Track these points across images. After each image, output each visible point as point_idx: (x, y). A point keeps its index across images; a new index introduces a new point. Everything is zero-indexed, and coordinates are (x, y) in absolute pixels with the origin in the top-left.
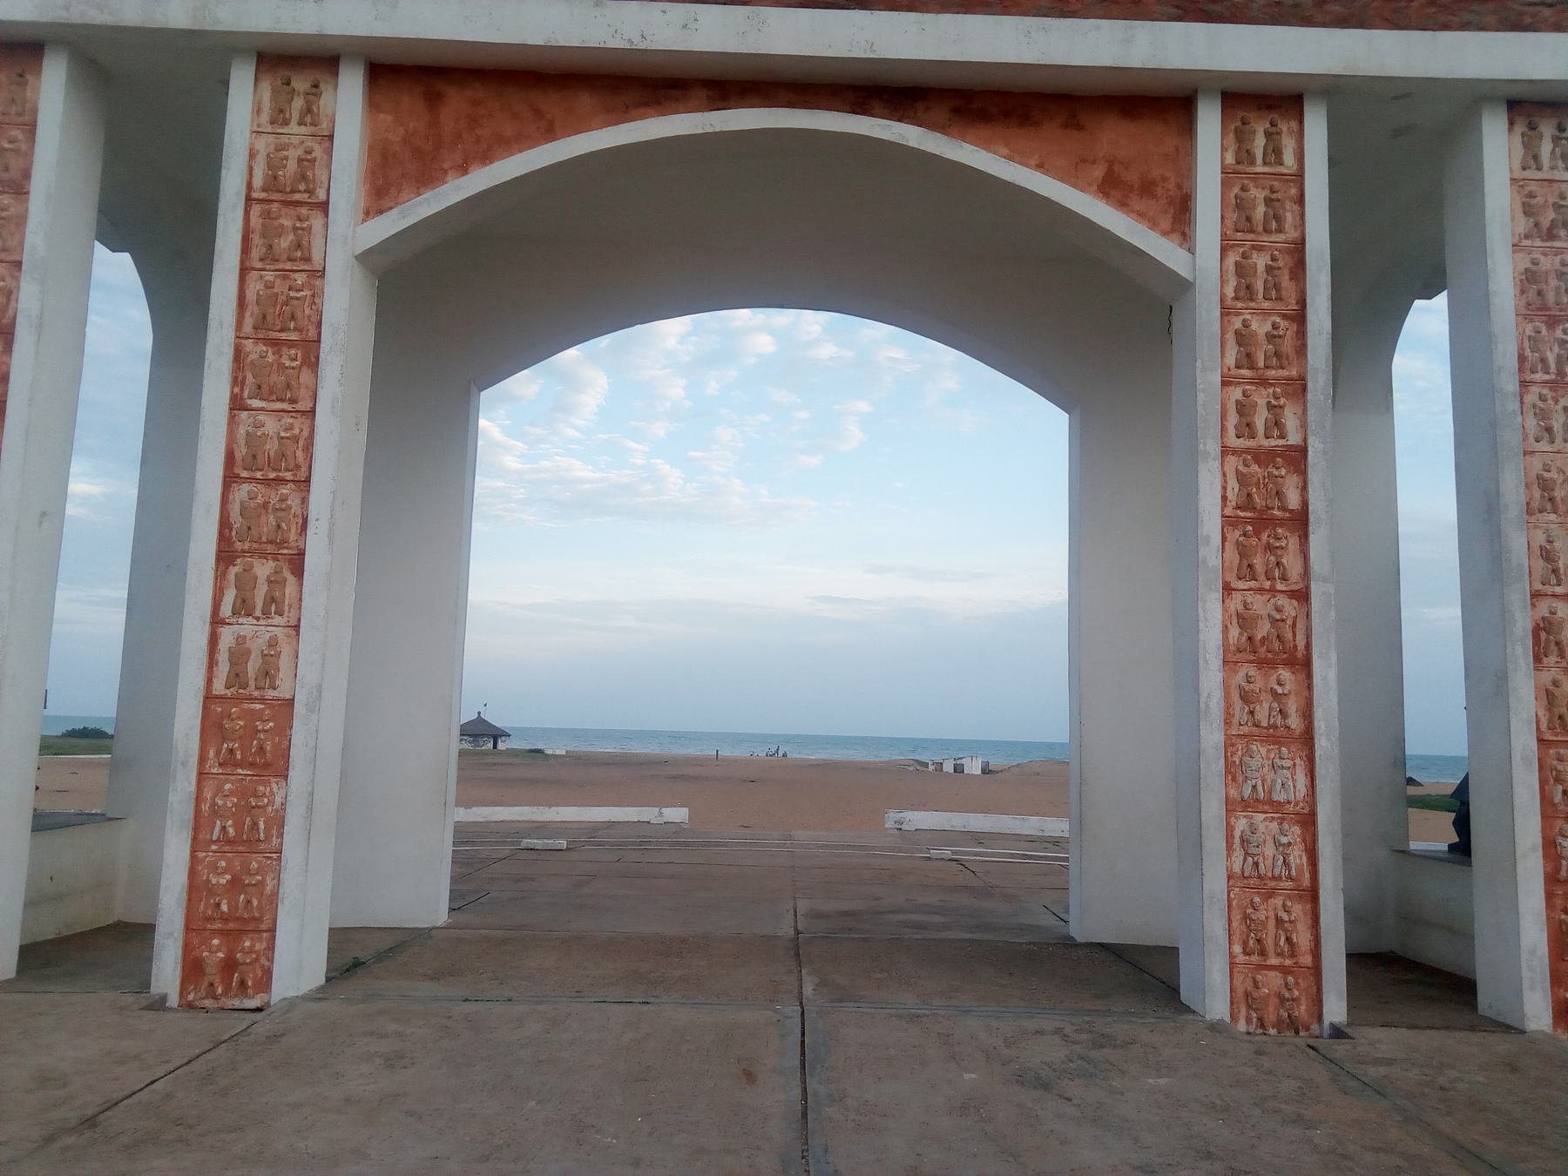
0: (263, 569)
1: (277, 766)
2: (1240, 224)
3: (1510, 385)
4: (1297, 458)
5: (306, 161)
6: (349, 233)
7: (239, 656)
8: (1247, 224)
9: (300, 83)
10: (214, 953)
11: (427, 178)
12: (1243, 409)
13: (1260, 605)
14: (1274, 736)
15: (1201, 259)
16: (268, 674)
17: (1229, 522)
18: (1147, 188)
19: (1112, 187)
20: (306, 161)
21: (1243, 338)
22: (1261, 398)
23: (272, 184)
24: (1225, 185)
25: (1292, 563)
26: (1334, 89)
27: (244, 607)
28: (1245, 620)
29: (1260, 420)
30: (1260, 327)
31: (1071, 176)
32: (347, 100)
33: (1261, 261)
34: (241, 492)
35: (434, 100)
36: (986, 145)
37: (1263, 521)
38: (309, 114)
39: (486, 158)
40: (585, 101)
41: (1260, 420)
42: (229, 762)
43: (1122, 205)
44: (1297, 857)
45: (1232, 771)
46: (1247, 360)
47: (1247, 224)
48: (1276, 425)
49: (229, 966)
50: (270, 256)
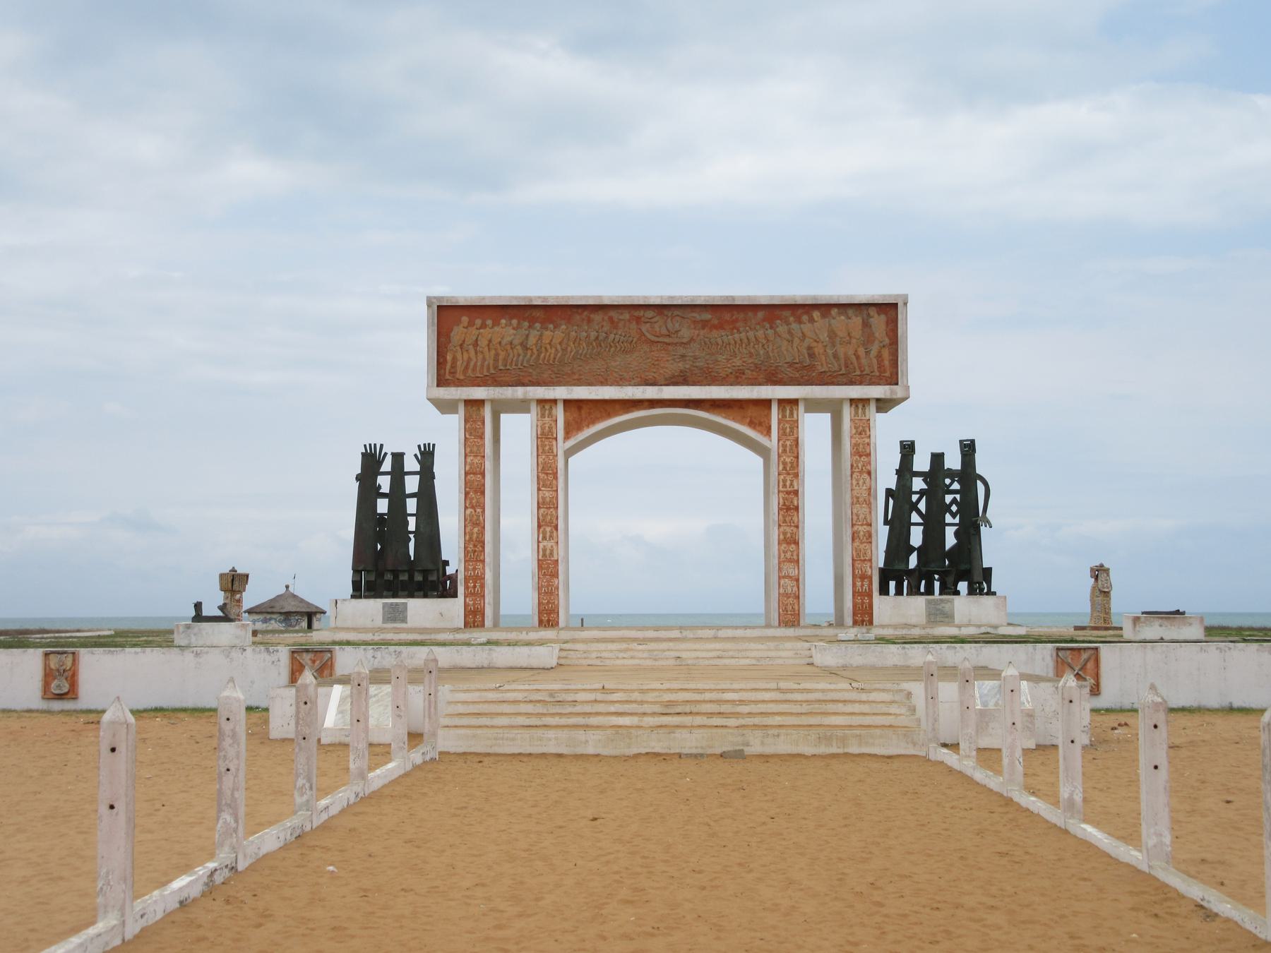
0: (548, 529)
1: (556, 575)
2: (783, 434)
3: (849, 473)
4: (796, 493)
5: (550, 428)
6: (562, 446)
7: (544, 550)
8: (784, 433)
9: (547, 407)
10: (545, 618)
11: (579, 428)
12: (785, 481)
13: (788, 530)
14: (790, 561)
15: (773, 442)
16: (551, 554)
17: (780, 509)
18: (760, 424)
19: (752, 424)
20: (550, 428)
21: (785, 464)
22: (789, 478)
23: (543, 433)
24: (779, 424)
25: (795, 519)
26: (805, 400)
27: (544, 538)
28: (785, 533)
29: (788, 483)
30: (788, 460)
31: (741, 422)
32: (560, 412)
33: (788, 443)
34: (542, 511)
35: (580, 408)
36: (719, 414)
37: (788, 509)
38: (550, 415)
39: (593, 422)
40: (617, 407)
41: (788, 483)
42: (545, 575)
43: (754, 428)
44: (795, 589)
45: (780, 569)
46: (785, 468)
47: (784, 433)
48: (791, 485)
49: (549, 621)
50: (544, 451)
